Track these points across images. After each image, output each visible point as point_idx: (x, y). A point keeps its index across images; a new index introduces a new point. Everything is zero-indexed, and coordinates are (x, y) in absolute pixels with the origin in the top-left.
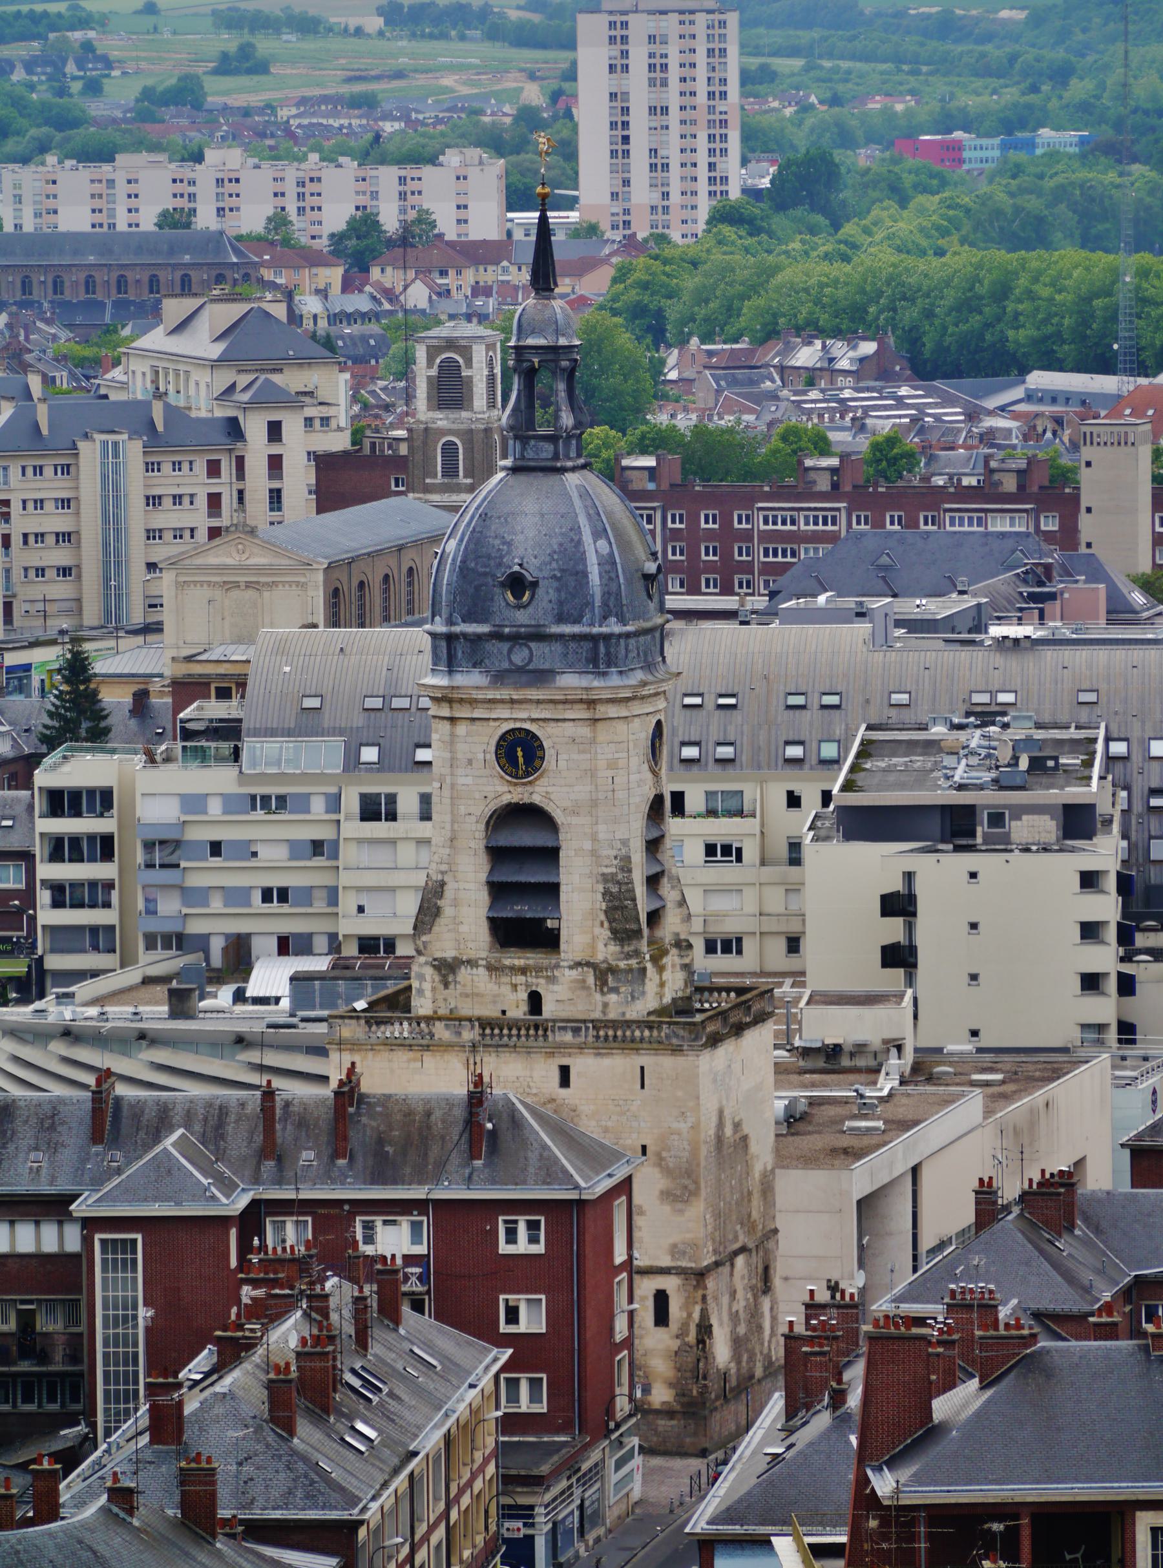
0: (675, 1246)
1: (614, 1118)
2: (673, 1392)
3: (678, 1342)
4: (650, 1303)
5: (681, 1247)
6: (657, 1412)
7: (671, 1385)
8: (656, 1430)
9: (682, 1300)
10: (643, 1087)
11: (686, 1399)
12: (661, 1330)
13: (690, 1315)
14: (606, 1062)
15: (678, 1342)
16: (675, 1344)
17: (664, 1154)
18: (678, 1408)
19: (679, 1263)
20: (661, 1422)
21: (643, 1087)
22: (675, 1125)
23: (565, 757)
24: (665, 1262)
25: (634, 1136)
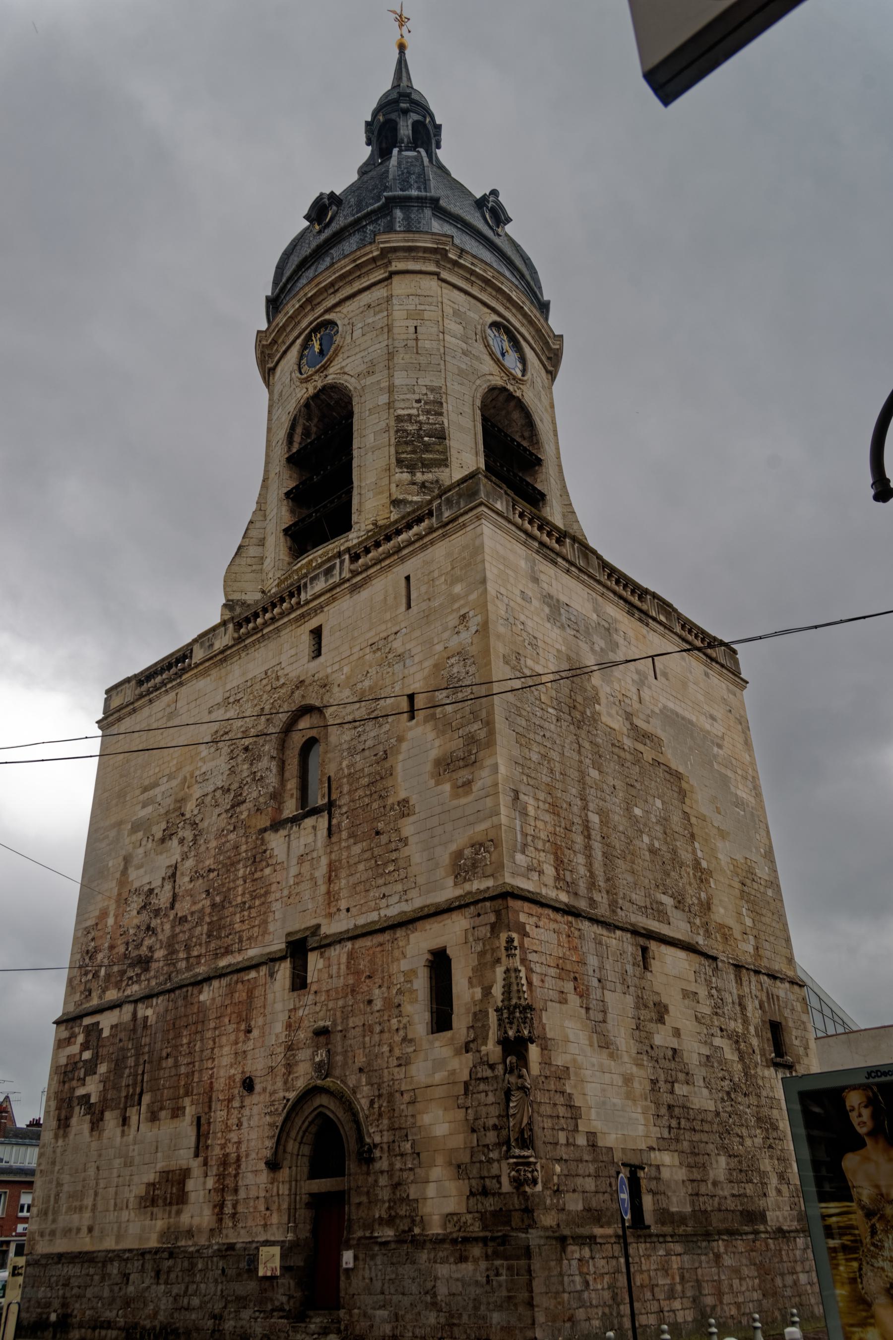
0: (459, 854)
1: (373, 671)
3: (469, 1059)
4: (421, 984)
7: (460, 1170)
9: (473, 961)
10: (409, 606)
13: (487, 992)
14: (364, 594)
15: (469, 1059)
16: (462, 1066)
18: (476, 1229)
19: (467, 887)
20: (443, 1270)
21: (409, 606)
22: (454, 642)
23: (360, 325)
24: (448, 892)
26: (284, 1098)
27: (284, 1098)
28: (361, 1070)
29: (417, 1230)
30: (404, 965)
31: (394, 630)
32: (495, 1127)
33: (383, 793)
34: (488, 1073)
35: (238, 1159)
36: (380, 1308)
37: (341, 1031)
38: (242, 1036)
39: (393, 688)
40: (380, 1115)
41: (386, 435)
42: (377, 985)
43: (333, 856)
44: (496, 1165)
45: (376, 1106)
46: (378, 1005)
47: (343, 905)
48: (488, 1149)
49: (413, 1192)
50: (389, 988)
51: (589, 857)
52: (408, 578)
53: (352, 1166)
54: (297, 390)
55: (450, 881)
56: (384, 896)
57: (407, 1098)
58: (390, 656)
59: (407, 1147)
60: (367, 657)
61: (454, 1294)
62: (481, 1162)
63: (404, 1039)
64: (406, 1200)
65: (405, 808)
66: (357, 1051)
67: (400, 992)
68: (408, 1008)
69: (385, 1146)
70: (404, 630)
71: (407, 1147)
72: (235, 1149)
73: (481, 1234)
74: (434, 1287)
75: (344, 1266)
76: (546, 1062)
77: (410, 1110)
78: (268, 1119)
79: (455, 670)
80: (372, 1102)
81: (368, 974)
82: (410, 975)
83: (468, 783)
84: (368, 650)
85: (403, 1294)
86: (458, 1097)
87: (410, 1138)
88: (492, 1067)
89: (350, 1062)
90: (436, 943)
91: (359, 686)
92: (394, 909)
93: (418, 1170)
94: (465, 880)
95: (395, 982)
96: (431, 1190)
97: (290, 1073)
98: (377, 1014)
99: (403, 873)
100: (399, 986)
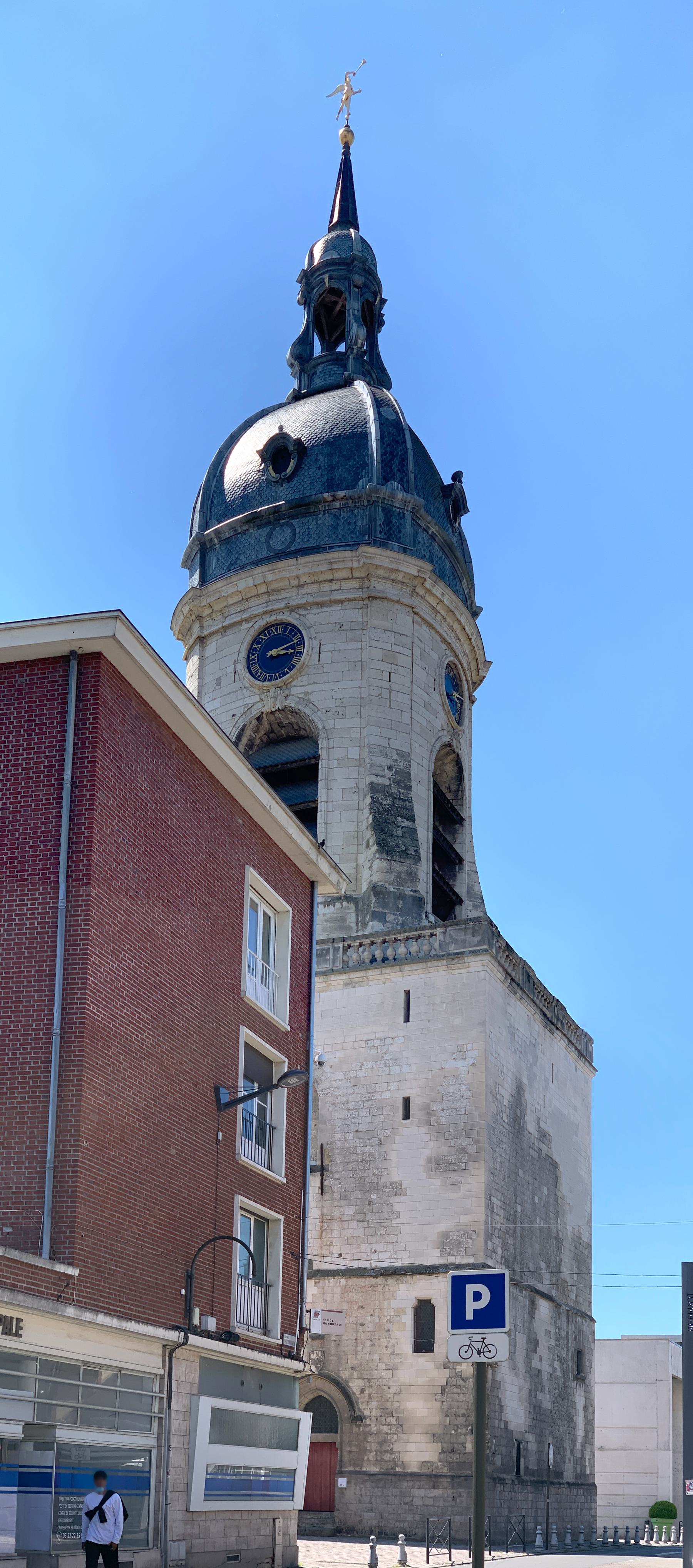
0: (445, 1235)
1: (368, 1065)
2: (438, 1447)
3: (447, 1373)
4: (408, 1320)
5: (454, 1235)
6: (413, 1475)
8: (411, 1503)
10: (407, 1020)
11: (455, 1458)
12: (424, 1358)
15: (447, 1373)
16: (442, 1377)
17: (434, 1107)
21: (407, 1020)
24: (433, 1258)
25: (393, 1087)
28: (352, 1368)
29: (398, 1469)
30: (394, 1304)
31: (393, 1035)
32: (464, 1415)
33: (377, 1172)
34: (461, 1382)
36: (368, 1511)
37: (335, 1341)
39: (388, 1086)
40: (370, 1398)
41: (355, 796)
42: (369, 1314)
43: (325, 1210)
44: (463, 1437)
45: (367, 1392)
46: (370, 1327)
47: (336, 1250)
48: (458, 1427)
49: (396, 1447)
50: (379, 1317)
51: (515, 1239)
52: (407, 993)
53: (345, 1426)
54: (246, 693)
55: (437, 1252)
56: (375, 1251)
57: (392, 1390)
58: (386, 1057)
59: (393, 1420)
60: (362, 1050)
61: (427, 1506)
62: (451, 1434)
63: (392, 1353)
64: (391, 1452)
65: (398, 1190)
66: (350, 1357)
67: (389, 1321)
68: (396, 1333)
69: (374, 1419)
70: (402, 1040)
71: (393, 1420)
73: (449, 1474)
74: (412, 1501)
75: (339, 1486)
76: (494, 1380)
77: (396, 1397)
79: (451, 1089)
80: (362, 1391)
81: (360, 1304)
82: (399, 1312)
83: (457, 1184)
84: (363, 1044)
85: (388, 1504)
86: (436, 1394)
88: (464, 1380)
89: (343, 1362)
90: (424, 1295)
91: (353, 1074)
92: (384, 1260)
94: (449, 1255)
95: (386, 1314)
96: (411, 1447)
98: (369, 1334)
99: (394, 1239)
100: (389, 1318)
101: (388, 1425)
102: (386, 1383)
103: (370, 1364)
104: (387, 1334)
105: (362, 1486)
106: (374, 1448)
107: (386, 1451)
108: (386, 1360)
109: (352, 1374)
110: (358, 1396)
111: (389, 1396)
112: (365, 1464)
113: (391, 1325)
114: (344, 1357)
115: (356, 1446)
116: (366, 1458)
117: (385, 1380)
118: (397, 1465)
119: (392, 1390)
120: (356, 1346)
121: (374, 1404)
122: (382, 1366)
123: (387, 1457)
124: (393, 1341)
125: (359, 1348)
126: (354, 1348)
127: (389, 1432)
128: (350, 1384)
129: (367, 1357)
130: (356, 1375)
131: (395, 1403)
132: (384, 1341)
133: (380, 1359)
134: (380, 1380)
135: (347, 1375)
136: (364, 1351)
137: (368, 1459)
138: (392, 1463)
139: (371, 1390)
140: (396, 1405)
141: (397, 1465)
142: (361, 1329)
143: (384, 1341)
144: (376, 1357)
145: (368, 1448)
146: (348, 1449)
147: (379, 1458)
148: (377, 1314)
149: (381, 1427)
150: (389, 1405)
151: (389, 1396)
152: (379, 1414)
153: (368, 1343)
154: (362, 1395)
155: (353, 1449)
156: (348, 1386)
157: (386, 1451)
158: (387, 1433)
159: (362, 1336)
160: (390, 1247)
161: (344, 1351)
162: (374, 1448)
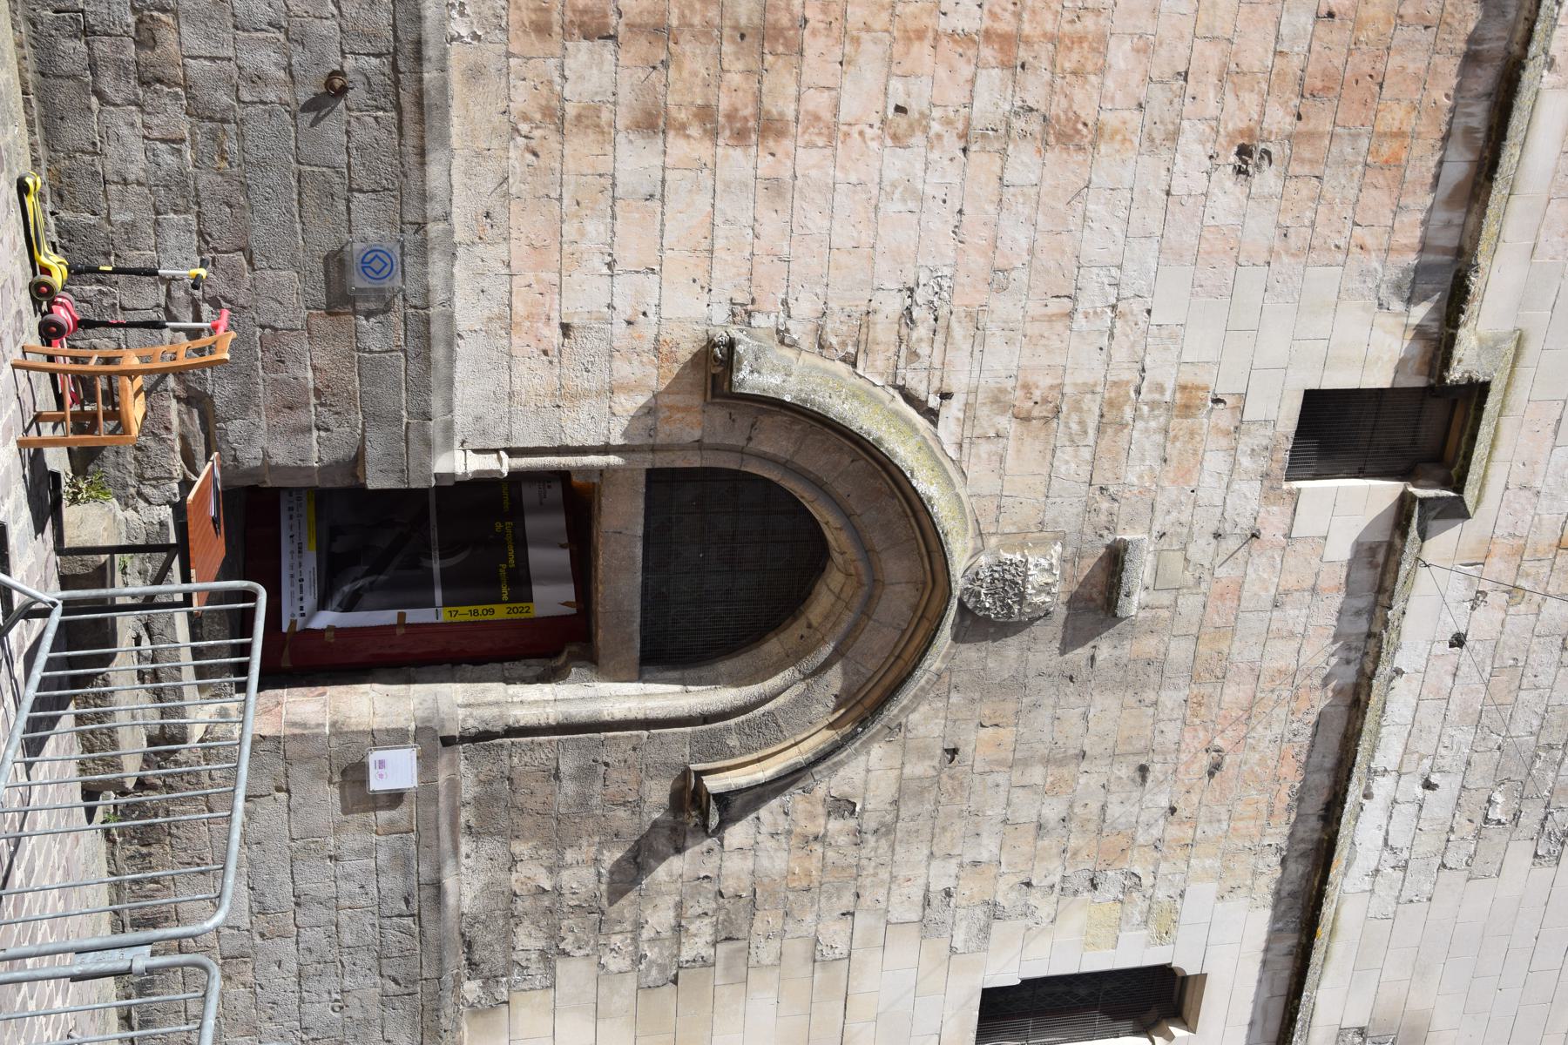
26: (946, 396)
27: (946, 396)
35: (768, 127)
38: (1239, 114)
45: (835, 825)
49: (574, 973)
57: (834, 933)
59: (698, 943)
63: (995, 912)
64: (552, 955)
66: (1007, 734)
68: (1080, 914)
71: (698, 943)
72: (817, 101)
77: (797, 949)
78: (893, 305)
80: (843, 806)
87: (723, 948)
89: (985, 709)
93: (631, 982)
97: (1026, 419)
98: (1095, 807)
100: (1147, 881)
101: (678, 928)
102: (867, 900)
103: (959, 826)
104: (1081, 881)
105: (383, 857)
106: (567, 878)
107: (554, 935)
108: (970, 889)
109: (924, 753)
110: (820, 791)
111: (810, 918)
112: (489, 846)
113: (1115, 891)
114: (1010, 706)
115: (583, 802)
116: (519, 848)
117: (881, 894)
118: (490, 980)
119: (834, 933)
120: (1047, 761)
121: (776, 861)
122: (942, 876)
123: (528, 940)
124: (1044, 906)
125: (1037, 774)
126: (1042, 750)
127: (646, 934)
128: (877, 750)
129: (995, 811)
130: (919, 769)
131: (775, 944)
132: (1050, 871)
133: (976, 863)
134: (884, 874)
135: (921, 731)
136: (1019, 796)
137: (514, 861)
138: (500, 959)
139: (843, 840)
140: (766, 952)
141: (490, 980)
142: (1126, 771)
143: (1050, 871)
144: (987, 849)
145: (570, 855)
146: (567, 766)
147: (520, 906)
148: (1174, 832)
149: (671, 900)
150: (767, 919)
151: (810, 918)
152: (729, 886)
153: (1052, 810)
154: (820, 810)
155: (569, 787)
156: (872, 739)
157: (554, 935)
158: (639, 926)
159: (1088, 781)
160: (1428, 843)
161: (1036, 706)
162: (567, 878)
